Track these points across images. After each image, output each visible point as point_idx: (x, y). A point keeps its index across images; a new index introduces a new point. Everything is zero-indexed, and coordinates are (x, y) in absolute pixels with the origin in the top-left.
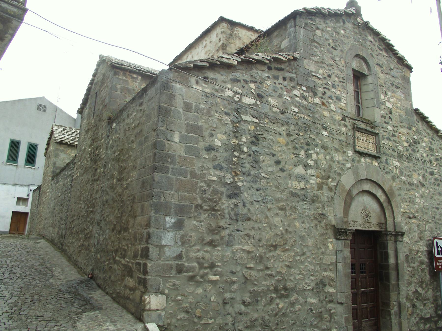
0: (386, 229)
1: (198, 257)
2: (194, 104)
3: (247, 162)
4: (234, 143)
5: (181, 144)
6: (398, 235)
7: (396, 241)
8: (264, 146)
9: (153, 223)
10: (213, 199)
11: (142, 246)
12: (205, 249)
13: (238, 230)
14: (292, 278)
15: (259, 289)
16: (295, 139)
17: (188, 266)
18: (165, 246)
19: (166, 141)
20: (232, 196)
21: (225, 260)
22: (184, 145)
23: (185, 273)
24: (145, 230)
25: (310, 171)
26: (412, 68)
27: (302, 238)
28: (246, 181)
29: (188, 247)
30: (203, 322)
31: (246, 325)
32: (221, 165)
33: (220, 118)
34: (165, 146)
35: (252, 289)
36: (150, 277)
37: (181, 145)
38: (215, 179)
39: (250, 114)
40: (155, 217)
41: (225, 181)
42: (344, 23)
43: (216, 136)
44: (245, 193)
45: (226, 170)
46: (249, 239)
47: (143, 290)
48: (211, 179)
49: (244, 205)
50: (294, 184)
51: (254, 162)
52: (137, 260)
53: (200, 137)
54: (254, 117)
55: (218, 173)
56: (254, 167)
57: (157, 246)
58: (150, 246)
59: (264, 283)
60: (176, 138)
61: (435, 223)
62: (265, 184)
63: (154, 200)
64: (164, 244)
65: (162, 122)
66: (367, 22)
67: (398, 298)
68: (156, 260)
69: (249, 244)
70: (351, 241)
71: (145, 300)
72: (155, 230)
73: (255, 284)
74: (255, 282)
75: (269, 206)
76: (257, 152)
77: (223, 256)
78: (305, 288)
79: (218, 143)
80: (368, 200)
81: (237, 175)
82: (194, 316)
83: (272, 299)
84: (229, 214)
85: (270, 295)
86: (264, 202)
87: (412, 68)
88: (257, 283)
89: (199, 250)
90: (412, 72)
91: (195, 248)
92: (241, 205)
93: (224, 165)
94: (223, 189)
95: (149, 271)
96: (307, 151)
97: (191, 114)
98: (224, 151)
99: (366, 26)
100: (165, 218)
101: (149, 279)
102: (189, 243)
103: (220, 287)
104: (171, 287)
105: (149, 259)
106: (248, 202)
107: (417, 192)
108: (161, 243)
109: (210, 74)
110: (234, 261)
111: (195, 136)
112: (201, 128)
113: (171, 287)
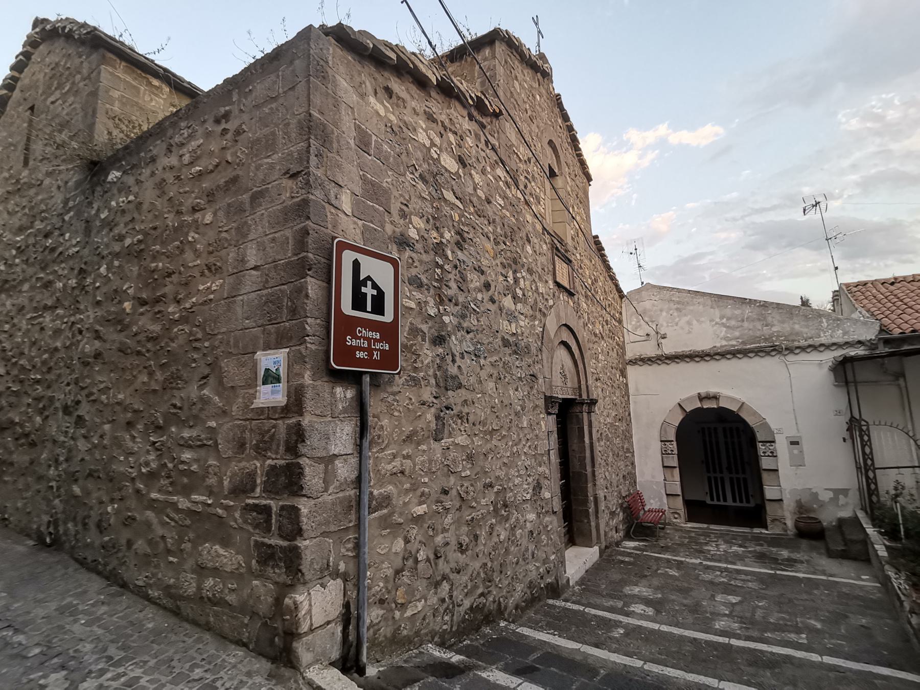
0: (580, 396)
1: (395, 470)
2: (374, 138)
3: (453, 279)
4: (435, 238)
5: (355, 219)
6: (593, 402)
7: (589, 413)
8: (471, 254)
9: (309, 405)
10: (412, 345)
11: (269, 462)
12: (404, 452)
13: (447, 408)
14: (511, 484)
15: (478, 516)
16: (502, 250)
17: (381, 494)
18: (335, 456)
19: (327, 205)
20: (437, 342)
21: (434, 470)
22: (360, 223)
23: (375, 512)
24: (280, 422)
25: (519, 306)
26: (592, 180)
27: (517, 414)
28: (453, 314)
29: (377, 452)
30: (409, 613)
31: (466, 591)
32: (419, 279)
33: (414, 184)
34: (327, 216)
35: (470, 517)
36: (307, 542)
37: (355, 223)
38: (413, 305)
39: (453, 190)
40: (314, 387)
41: (426, 310)
42: (539, 85)
43: (410, 219)
44: (453, 338)
45: (427, 290)
46: (462, 424)
47: (283, 578)
48: (407, 305)
49: (454, 361)
50: (506, 327)
51: (461, 281)
52: (249, 498)
53: (386, 213)
54: (457, 198)
55: (417, 295)
56: (462, 290)
57: (320, 460)
58: (303, 461)
59: (483, 502)
60: (346, 202)
61: (612, 386)
62: (475, 323)
63: (309, 345)
64: (335, 453)
65: (316, 156)
66: (559, 95)
67: (594, 490)
68: (319, 495)
69: (463, 433)
70: (557, 415)
71: (296, 608)
72: (315, 419)
73: (472, 507)
74: (474, 504)
75: (482, 361)
76: (464, 262)
77: (430, 461)
78: (524, 498)
79: (413, 234)
80: (562, 353)
81: (441, 302)
82: (393, 605)
83: (492, 527)
84: (435, 376)
85: (490, 522)
86: (476, 355)
87: (592, 180)
88: (475, 505)
89: (394, 456)
90: (590, 185)
91: (389, 452)
92: (449, 358)
93: (425, 281)
94: (425, 327)
95: (304, 527)
96: (515, 272)
97: (370, 158)
98: (422, 251)
99: (557, 101)
100: (333, 388)
101: (306, 547)
102: (378, 444)
103: (428, 528)
104: (350, 554)
105: (304, 496)
106: (457, 354)
107: (599, 346)
108: (328, 452)
109: (397, 86)
110: (446, 469)
111: (378, 209)
112: (386, 192)
113: (350, 554)
